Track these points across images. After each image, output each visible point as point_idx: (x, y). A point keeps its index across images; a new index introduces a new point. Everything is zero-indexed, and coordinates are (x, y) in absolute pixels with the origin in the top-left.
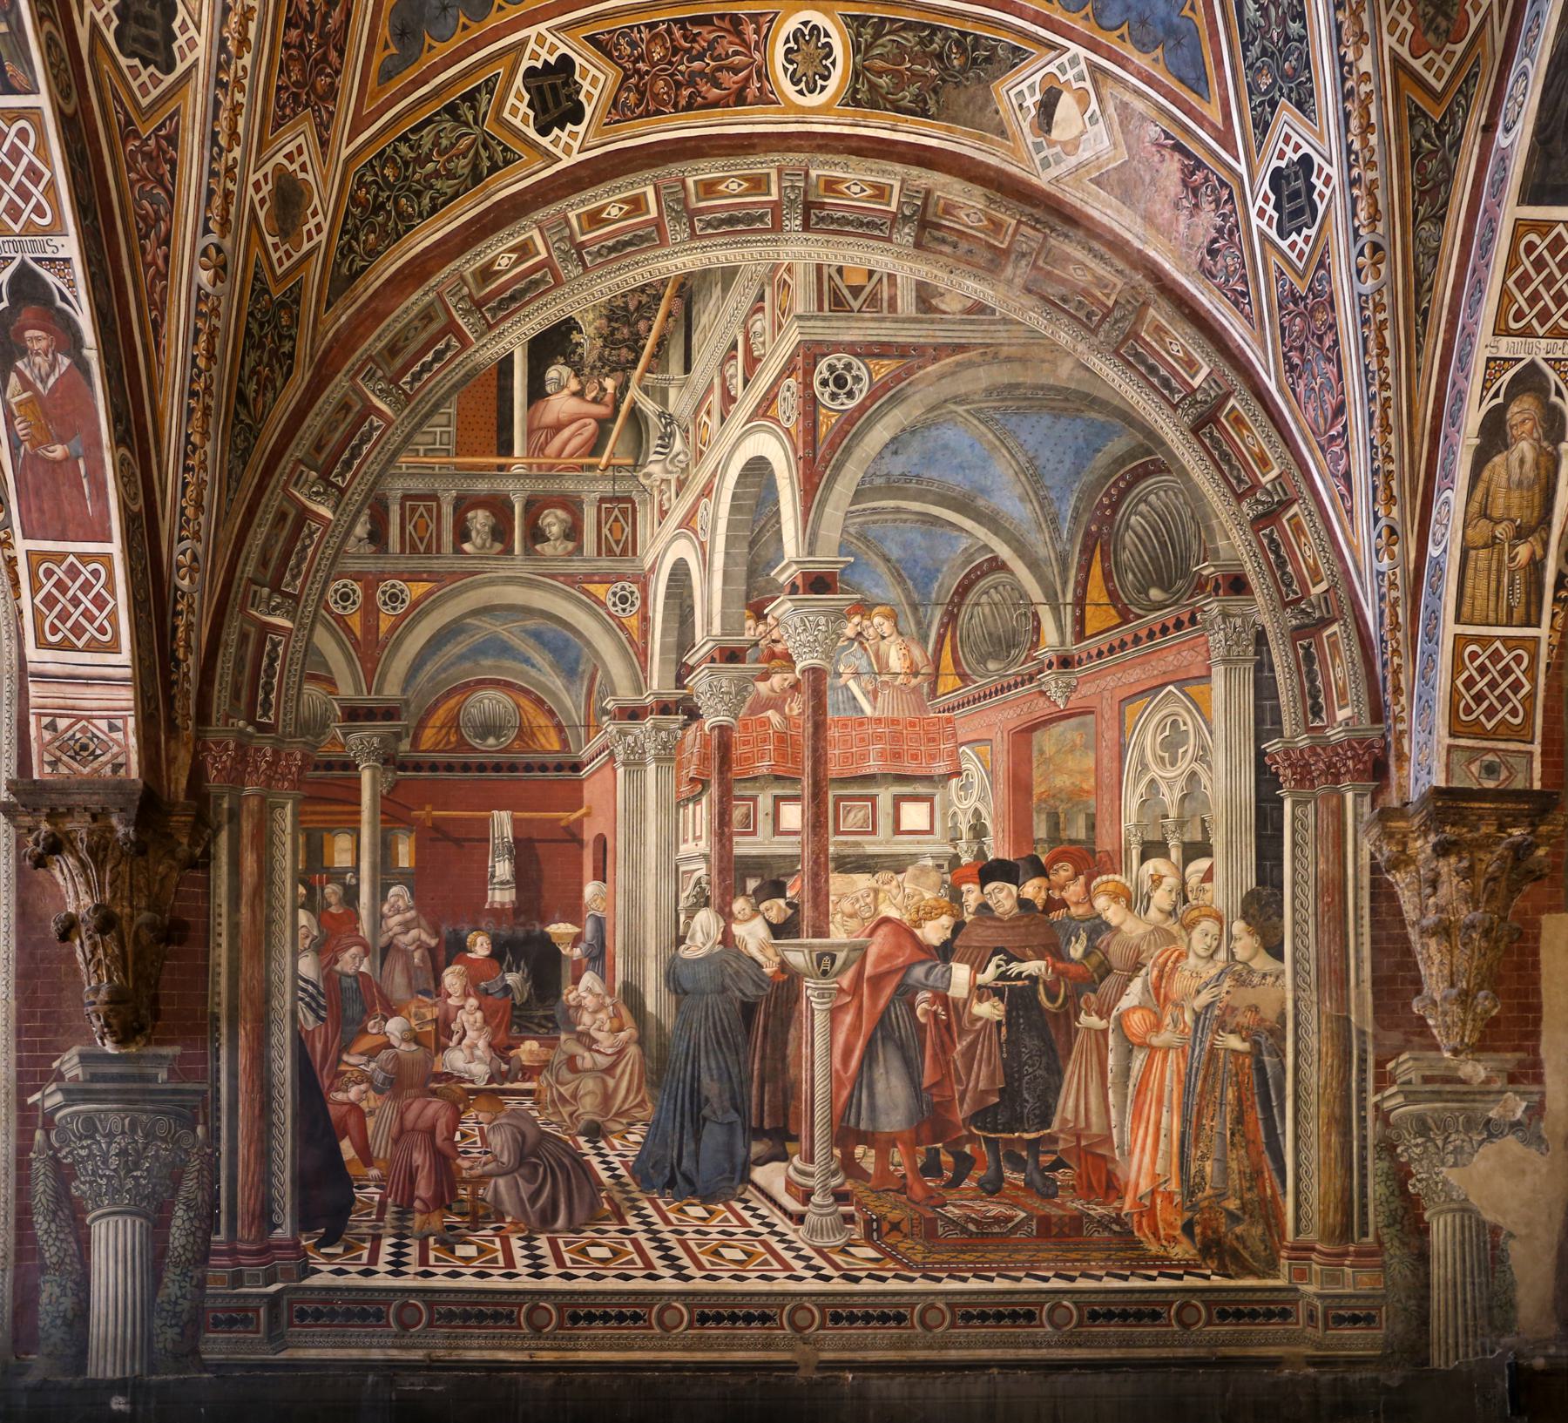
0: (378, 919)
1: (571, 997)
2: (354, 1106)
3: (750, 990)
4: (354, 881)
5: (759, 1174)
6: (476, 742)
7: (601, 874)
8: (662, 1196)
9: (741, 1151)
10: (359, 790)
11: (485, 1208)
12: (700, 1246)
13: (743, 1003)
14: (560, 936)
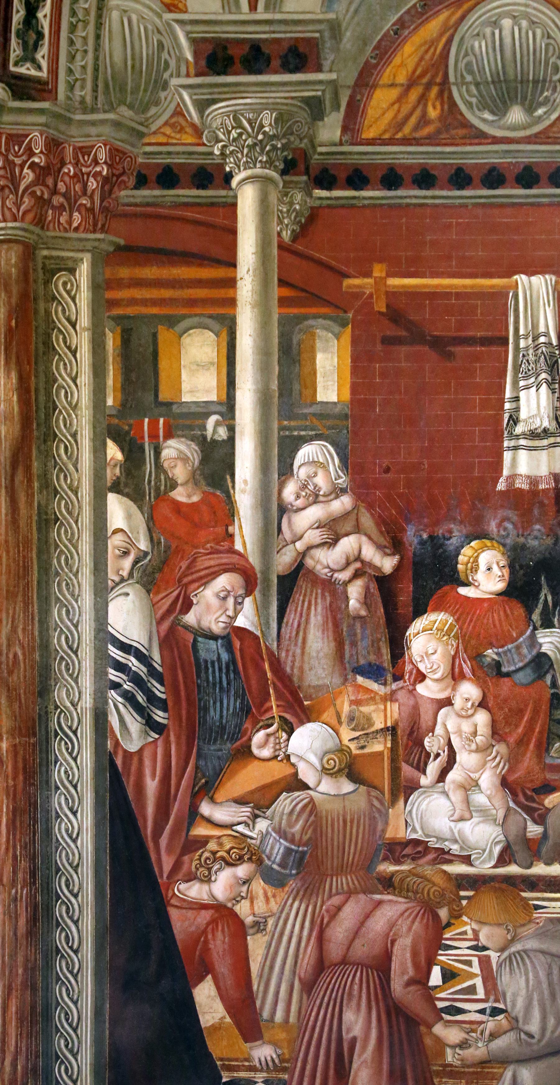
0: (274, 513)
2: (223, 913)
4: (222, 433)
6: (482, 120)
10: (232, 232)
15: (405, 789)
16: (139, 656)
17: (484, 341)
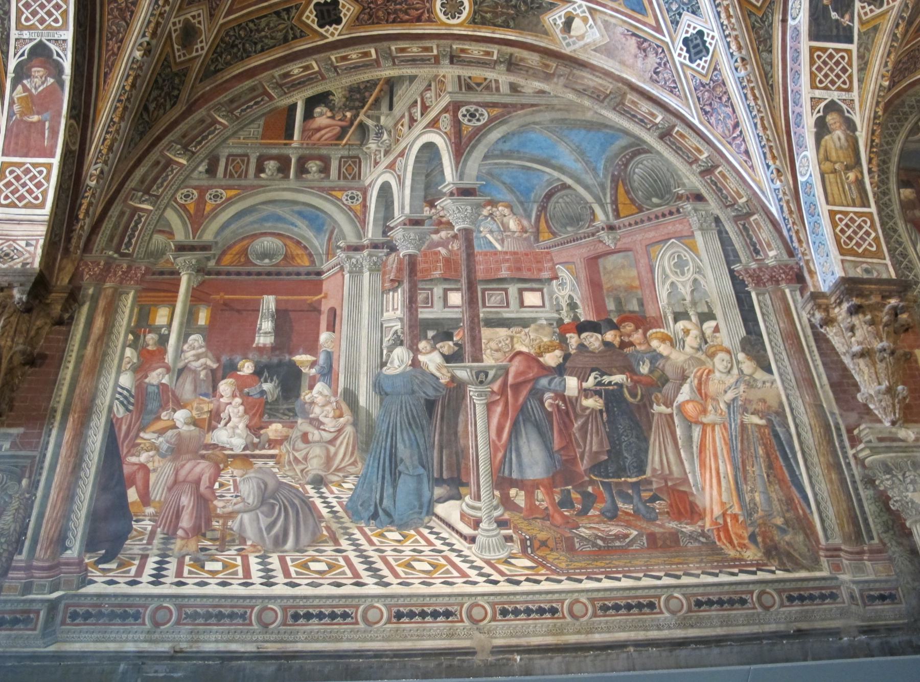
0: (179, 352)
1: (307, 397)
3: (431, 393)
5: (440, 509)
6: (258, 262)
7: (331, 327)
8: (368, 525)
9: (426, 494)
10: (179, 285)
11: (232, 535)
12: (396, 560)
13: (426, 400)
14: (302, 362)
15: (211, 428)
16: (127, 390)
17: (253, 310)
